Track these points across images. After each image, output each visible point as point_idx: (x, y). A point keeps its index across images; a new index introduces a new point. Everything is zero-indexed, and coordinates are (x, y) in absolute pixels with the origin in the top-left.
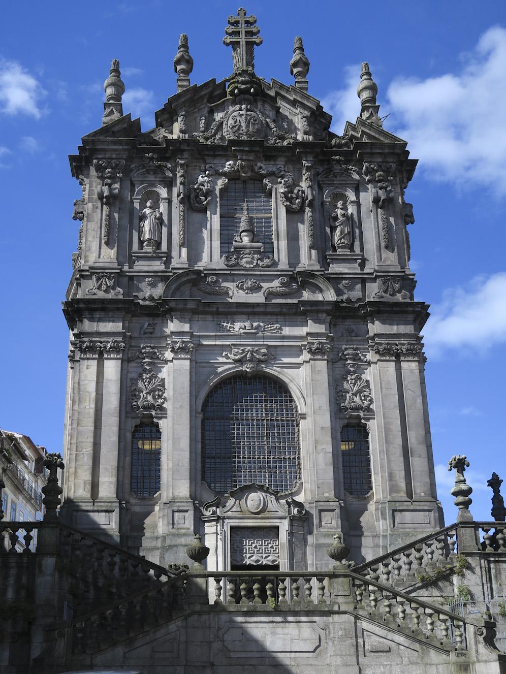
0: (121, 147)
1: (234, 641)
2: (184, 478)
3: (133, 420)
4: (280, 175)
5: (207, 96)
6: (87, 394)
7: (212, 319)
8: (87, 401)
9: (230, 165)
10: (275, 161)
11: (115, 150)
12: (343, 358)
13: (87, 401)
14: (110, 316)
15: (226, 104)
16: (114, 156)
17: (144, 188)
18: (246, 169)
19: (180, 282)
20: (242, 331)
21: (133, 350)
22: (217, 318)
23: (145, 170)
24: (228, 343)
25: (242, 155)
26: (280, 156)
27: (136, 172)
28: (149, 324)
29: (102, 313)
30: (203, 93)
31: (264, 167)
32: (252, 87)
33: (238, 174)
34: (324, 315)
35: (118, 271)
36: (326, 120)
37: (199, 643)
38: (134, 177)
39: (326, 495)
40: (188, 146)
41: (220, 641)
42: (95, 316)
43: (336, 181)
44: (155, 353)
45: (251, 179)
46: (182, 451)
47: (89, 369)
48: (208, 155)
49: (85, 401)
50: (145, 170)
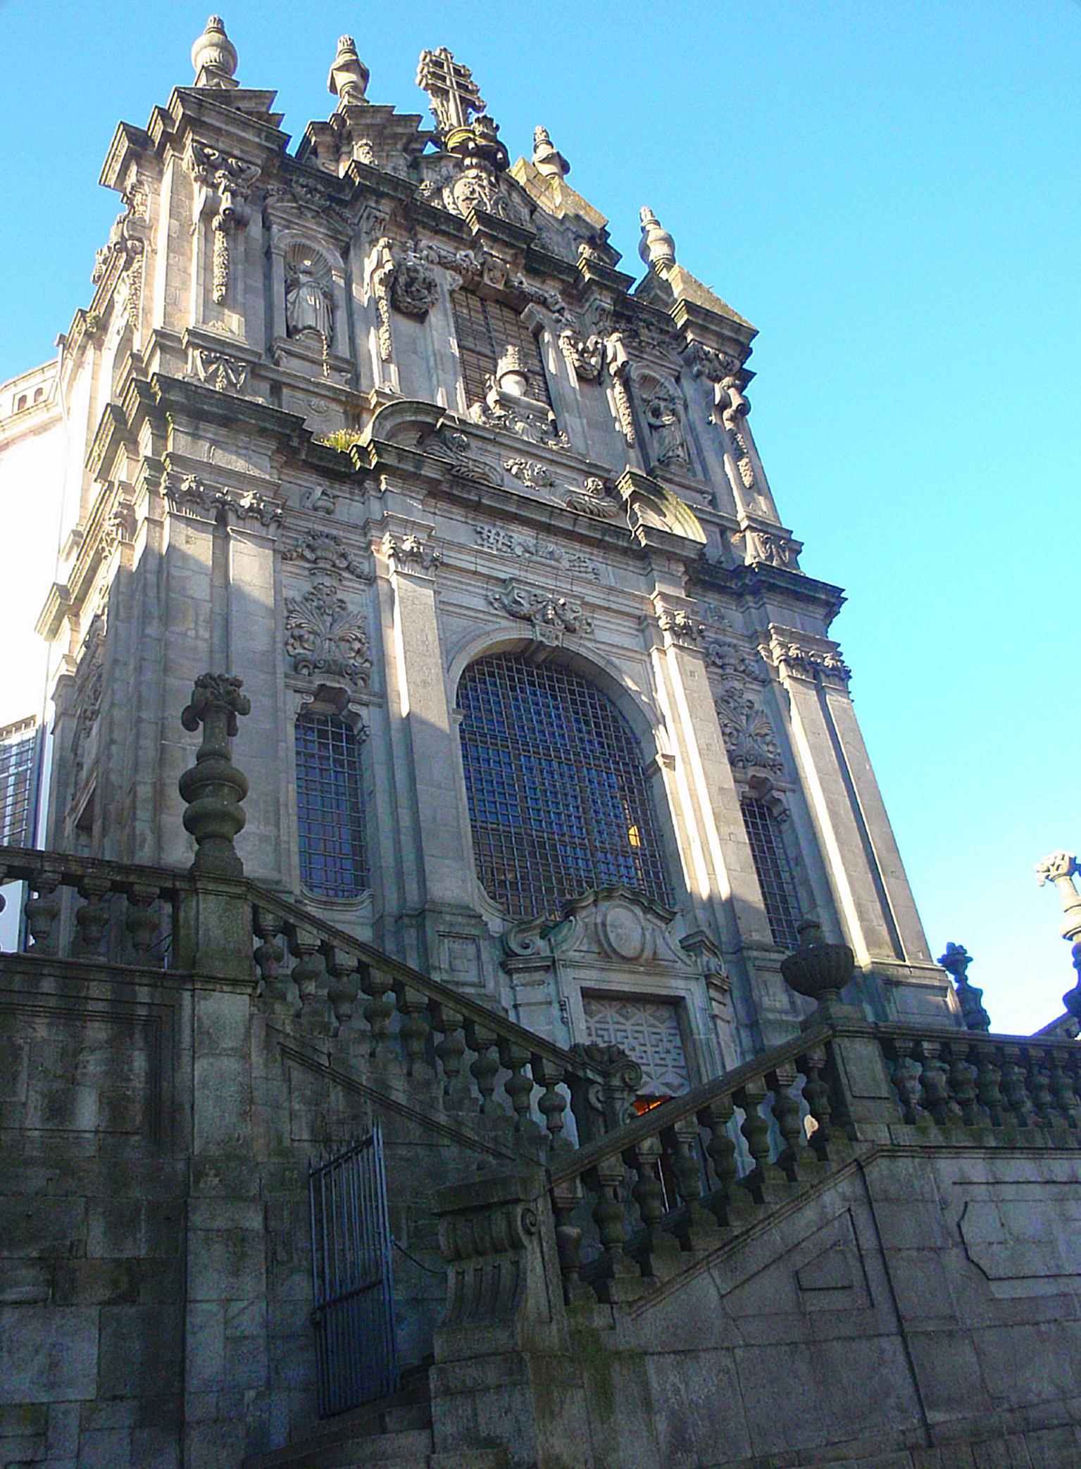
0: (257, 140)
1: (991, 1244)
2: (451, 854)
3: (298, 695)
4: (557, 307)
5: (404, 141)
6: (189, 600)
7: (463, 519)
8: (190, 618)
9: (466, 256)
10: (543, 282)
11: (242, 140)
12: (719, 662)
13: (190, 618)
14: (240, 444)
15: (443, 163)
16: (236, 152)
17: (293, 236)
18: (498, 274)
19: (399, 420)
20: (527, 555)
21: (289, 537)
22: (473, 519)
23: (294, 205)
24: (502, 576)
25: (492, 248)
26: (555, 278)
27: (278, 201)
28: (324, 493)
29: (223, 431)
30: (400, 130)
31: (525, 285)
32: (498, 150)
33: (477, 278)
34: (682, 569)
35: (256, 360)
36: (611, 259)
37: (914, 1254)
38: (273, 208)
39: (756, 936)
40: (396, 190)
41: (955, 1245)
42: (201, 433)
43: (651, 355)
44: (343, 556)
45: (497, 301)
46: (440, 787)
47: (193, 546)
48: (425, 226)
49: (184, 616)
50: (294, 205)
